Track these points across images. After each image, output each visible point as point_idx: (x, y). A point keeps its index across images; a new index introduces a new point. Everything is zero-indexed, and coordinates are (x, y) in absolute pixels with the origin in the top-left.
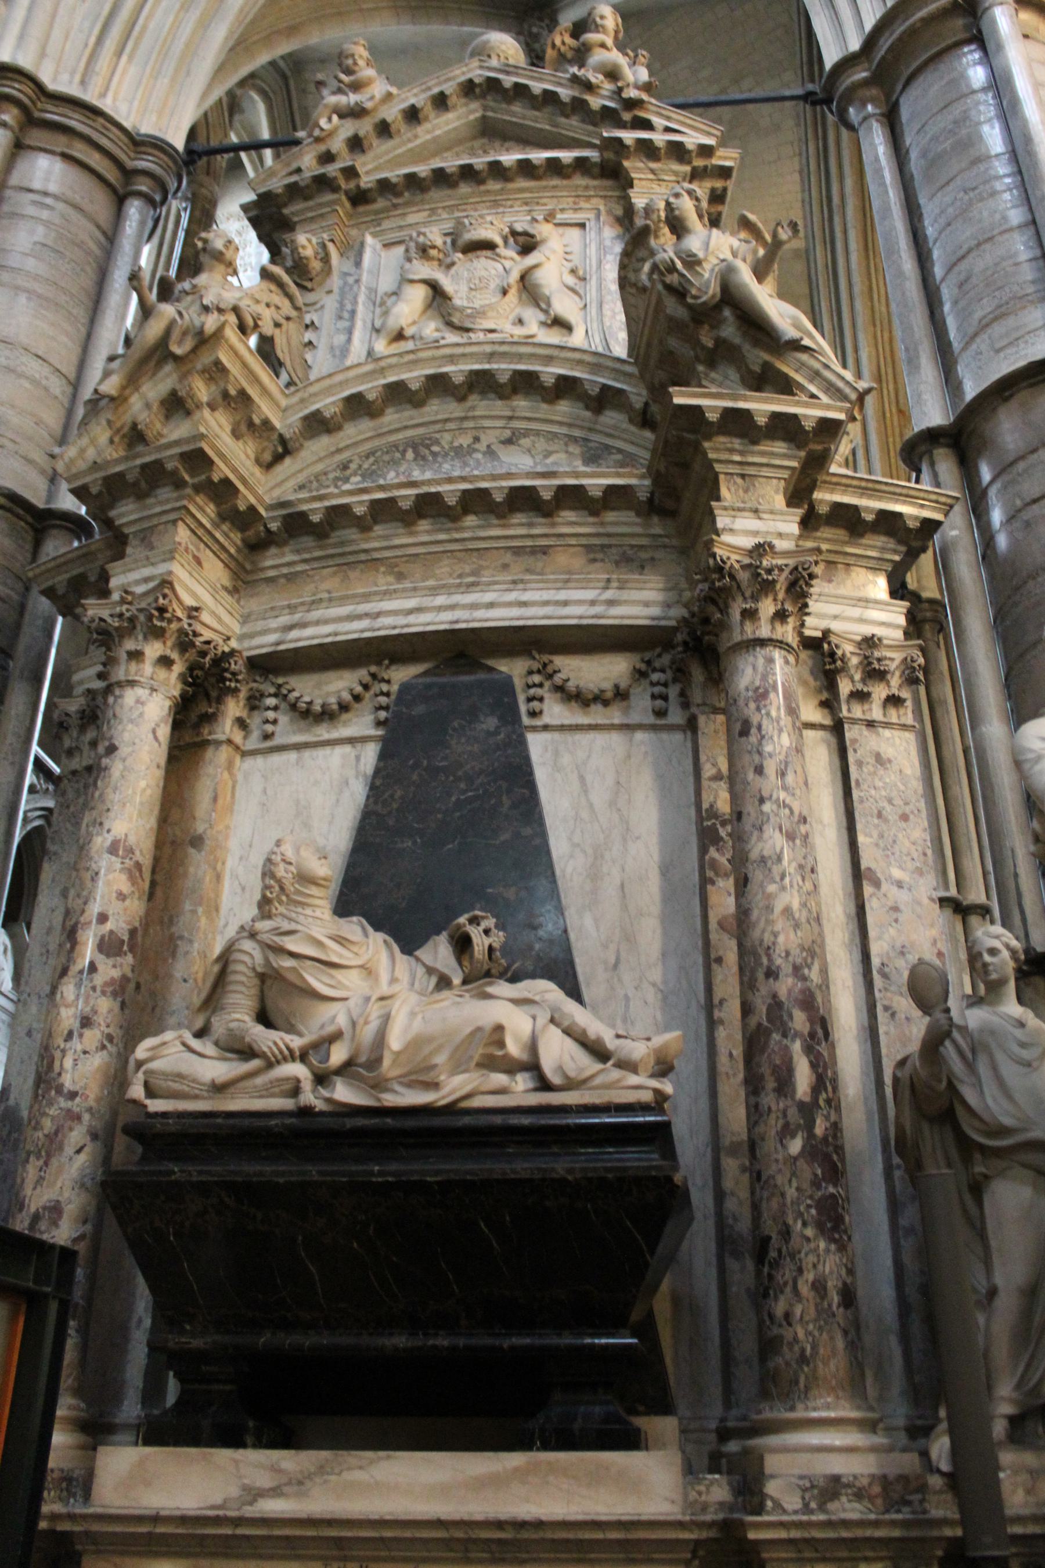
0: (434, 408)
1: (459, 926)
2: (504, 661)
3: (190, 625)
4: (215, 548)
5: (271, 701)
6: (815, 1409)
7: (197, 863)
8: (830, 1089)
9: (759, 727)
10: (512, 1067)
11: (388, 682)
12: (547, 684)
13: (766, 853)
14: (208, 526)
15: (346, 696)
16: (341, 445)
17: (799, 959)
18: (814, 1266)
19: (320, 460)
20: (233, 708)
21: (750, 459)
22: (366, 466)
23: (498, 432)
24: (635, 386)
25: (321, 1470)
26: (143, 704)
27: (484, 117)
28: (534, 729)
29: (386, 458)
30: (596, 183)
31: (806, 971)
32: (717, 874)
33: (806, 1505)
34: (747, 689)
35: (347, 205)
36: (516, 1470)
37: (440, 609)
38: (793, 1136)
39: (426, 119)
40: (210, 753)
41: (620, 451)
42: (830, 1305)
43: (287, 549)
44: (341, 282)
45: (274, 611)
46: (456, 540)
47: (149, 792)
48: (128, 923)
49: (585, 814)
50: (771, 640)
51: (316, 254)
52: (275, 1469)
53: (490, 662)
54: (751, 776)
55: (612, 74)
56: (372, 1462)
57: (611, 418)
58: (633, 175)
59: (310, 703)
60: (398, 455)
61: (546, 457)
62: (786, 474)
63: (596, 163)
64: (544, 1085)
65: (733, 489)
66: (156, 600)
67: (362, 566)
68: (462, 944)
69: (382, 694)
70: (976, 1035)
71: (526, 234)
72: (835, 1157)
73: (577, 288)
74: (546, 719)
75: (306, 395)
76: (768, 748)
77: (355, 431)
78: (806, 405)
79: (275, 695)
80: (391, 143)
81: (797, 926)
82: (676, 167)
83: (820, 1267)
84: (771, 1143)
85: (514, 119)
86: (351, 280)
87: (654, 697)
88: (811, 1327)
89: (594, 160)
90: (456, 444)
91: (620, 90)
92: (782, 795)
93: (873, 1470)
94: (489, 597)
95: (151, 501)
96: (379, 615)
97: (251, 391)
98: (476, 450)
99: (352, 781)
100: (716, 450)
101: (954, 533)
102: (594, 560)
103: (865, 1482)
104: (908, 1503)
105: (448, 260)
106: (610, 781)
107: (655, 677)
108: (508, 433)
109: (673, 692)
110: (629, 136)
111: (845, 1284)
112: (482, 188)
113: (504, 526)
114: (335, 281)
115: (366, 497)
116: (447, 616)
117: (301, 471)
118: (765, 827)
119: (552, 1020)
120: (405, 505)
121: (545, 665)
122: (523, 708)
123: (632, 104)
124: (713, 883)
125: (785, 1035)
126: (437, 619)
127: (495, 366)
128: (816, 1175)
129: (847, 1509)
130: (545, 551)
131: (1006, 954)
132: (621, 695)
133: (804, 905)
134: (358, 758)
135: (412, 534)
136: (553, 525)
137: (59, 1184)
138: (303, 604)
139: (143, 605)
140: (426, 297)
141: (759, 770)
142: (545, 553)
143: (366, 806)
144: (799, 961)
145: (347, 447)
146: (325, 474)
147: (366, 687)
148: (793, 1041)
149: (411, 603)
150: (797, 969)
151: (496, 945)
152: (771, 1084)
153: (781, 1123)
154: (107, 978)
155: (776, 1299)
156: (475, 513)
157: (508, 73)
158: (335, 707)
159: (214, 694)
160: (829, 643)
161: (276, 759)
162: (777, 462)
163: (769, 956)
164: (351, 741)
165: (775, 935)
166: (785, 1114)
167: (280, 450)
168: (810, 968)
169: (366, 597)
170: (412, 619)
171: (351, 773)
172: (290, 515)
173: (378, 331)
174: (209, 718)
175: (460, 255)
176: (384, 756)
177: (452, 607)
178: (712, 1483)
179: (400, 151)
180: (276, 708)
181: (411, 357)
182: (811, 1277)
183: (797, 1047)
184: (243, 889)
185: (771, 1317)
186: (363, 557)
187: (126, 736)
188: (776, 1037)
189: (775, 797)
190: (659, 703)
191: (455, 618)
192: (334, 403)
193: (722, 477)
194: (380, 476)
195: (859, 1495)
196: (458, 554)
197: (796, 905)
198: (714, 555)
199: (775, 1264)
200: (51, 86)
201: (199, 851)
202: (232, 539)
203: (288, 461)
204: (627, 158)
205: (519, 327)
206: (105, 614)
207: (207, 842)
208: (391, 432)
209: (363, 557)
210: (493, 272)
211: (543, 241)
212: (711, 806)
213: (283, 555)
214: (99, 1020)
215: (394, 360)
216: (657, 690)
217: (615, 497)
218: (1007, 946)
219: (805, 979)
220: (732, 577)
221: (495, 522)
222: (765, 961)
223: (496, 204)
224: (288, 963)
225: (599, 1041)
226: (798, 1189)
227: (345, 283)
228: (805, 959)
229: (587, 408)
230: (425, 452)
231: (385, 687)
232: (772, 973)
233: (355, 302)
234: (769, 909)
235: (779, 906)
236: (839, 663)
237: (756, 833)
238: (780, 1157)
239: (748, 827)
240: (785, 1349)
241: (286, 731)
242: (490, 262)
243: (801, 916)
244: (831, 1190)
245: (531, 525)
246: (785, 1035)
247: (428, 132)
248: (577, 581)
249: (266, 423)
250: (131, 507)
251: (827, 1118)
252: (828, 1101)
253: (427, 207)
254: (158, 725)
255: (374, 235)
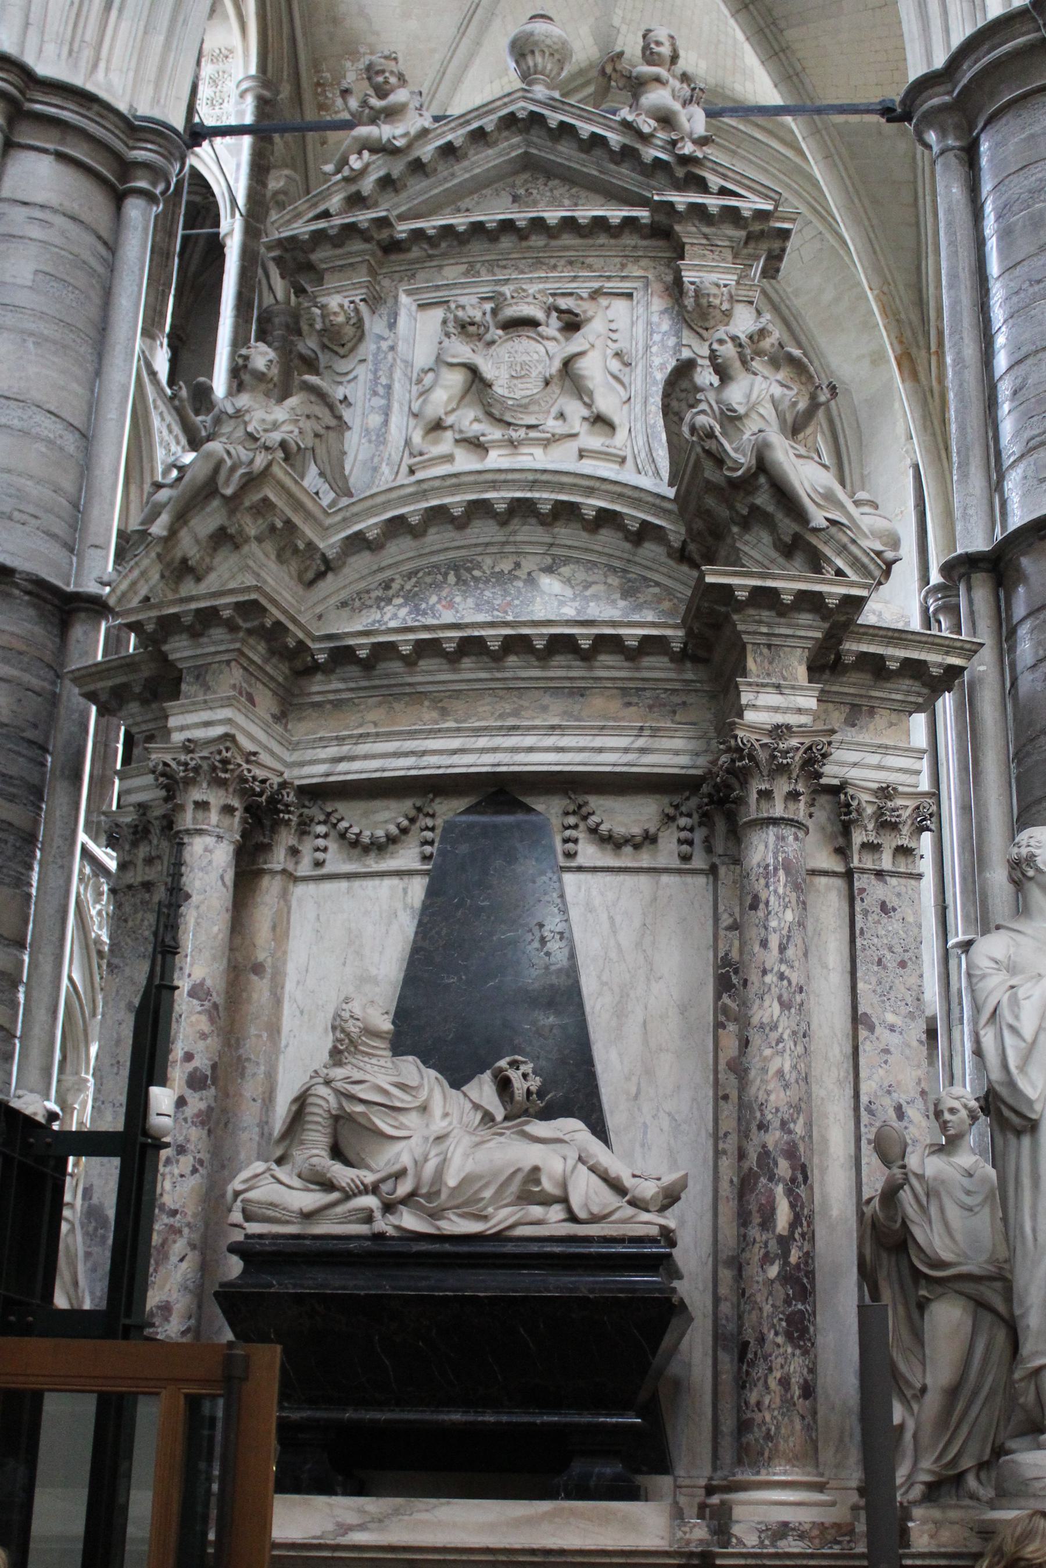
0: (476, 530)
1: (501, 1070)
2: (542, 799)
3: (249, 771)
4: (266, 680)
5: (321, 829)
6: (775, 1474)
7: (260, 989)
8: (805, 1223)
9: (767, 903)
10: (547, 1201)
11: (433, 816)
12: (582, 826)
13: (765, 1020)
14: (259, 661)
15: (393, 830)
16: (383, 564)
17: (785, 1113)
18: (782, 1367)
19: (363, 578)
20: (286, 838)
21: (777, 631)
22: (408, 587)
23: (538, 558)
24: (673, 523)
25: (397, 1512)
26: (211, 851)
27: (526, 153)
28: (569, 869)
29: (428, 579)
30: (645, 243)
31: (792, 1125)
32: (728, 1020)
33: (762, 1542)
34: (759, 866)
35: (379, 253)
36: (546, 1513)
37: (483, 751)
38: (772, 1263)
39: (465, 156)
40: (266, 881)
41: (657, 584)
42: (792, 1397)
43: (332, 677)
44: (373, 347)
45: (323, 742)
46: (498, 679)
47: (220, 936)
48: (210, 1059)
49: (613, 955)
50: (783, 819)
51: (349, 319)
52: (361, 1511)
53: (528, 800)
54: (757, 948)
55: (666, 120)
56: (435, 1507)
57: (651, 550)
58: (685, 240)
59: (358, 835)
60: (440, 577)
61: (586, 588)
62: (809, 644)
63: (645, 225)
64: (573, 1218)
65: (758, 660)
66: (220, 752)
67: (407, 699)
68: (504, 1085)
69: (427, 828)
70: (930, 1182)
71: (569, 312)
72: (805, 1281)
73: (621, 376)
74: (580, 860)
75: (348, 514)
76: (773, 924)
77: (400, 549)
78: (831, 582)
79: (325, 822)
80: (425, 183)
81: (786, 1086)
82: (731, 231)
83: (786, 1367)
84: (753, 1270)
85: (559, 160)
86: (385, 345)
87: (680, 842)
88: (776, 1413)
89: (643, 221)
90: (497, 569)
91: (674, 143)
92: (783, 968)
93: (817, 1520)
94: (529, 741)
95: (205, 640)
96: (424, 753)
97: (296, 520)
98: (517, 578)
99: (400, 913)
100: (744, 622)
101: (982, 668)
102: (629, 704)
103: (807, 1527)
104: (839, 1543)
105: (488, 337)
106: (637, 923)
107: (683, 821)
108: (549, 560)
109: (698, 836)
110: (681, 200)
111: (806, 1381)
112: (524, 244)
113: (543, 668)
114: (368, 348)
115: (411, 636)
116: (489, 758)
117: (345, 587)
118: (766, 997)
119: (580, 1159)
120: (450, 647)
121: (580, 807)
122: (559, 847)
123: (686, 160)
124: (724, 1027)
125: (771, 1179)
126: (479, 762)
127: (537, 495)
128: (788, 1295)
129: (791, 1545)
130: (582, 692)
131: (964, 1113)
132: (650, 839)
133: (794, 1067)
134: (405, 891)
135: (455, 671)
136: (591, 668)
137: (168, 1287)
138: (350, 737)
139: (205, 754)
140: (465, 382)
141: (764, 944)
142: (582, 695)
143: (415, 941)
144: (786, 1116)
145: (390, 566)
146: (368, 592)
147: (412, 821)
148: (777, 1184)
149: (455, 743)
150: (784, 1124)
151: (533, 1089)
152: (756, 1219)
153: (763, 1251)
154: (196, 1111)
155: (751, 1390)
156: (516, 654)
157: (554, 109)
158: (383, 840)
159: (267, 822)
160: (846, 794)
161: (328, 886)
162: (802, 633)
163: (761, 1111)
164: (399, 873)
165: (768, 1093)
166: (766, 1244)
167: (323, 568)
168: (795, 1122)
169: (412, 734)
170: (456, 759)
171: (399, 905)
172: (337, 648)
173: (416, 416)
174: (265, 848)
175: (500, 332)
176: (431, 892)
177: (495, 750)
178: (695, 1526)
179: (436, 191)
180: (326, 836)
181: (454, 481)
182: (778, 1374)
183: (780, 1190)
184: (302, 1012)
185: (746, 1403)
186: (408, 690)
187: (197, 884)
188: (763, 1180)
189: (776, 969)
190: (685, 848)
191: (496, 761)
192: (376, 524)
193: (749, 647)
194: (422, 599)
195: (802, 1536)
196: (501, 693)
197: (787, 1068)
198: (736, 737)
199: (752, 1364)
200: (43, 70)
201: (262, 978)
202: (279, 671)
203: (330, 576)
204: (679, 222)
205: (560, 422)
206: (168, 758)
207: (269, 970)
208: (432, 553)
209: (408, 690)
210: (536, 357)
211: (589, 320)
212: (727, 954)
213: (330, 682)
214: (191, 1147)
215: (437, 483)
216: (684, 835)
217: (650, 645)
218: (965, 1106)
219: (790, 1132)
220: (752, 757)
221: (536, 663)
222: (758, 1114)
223: (538, 263)
224: (360, 1108)
225: (618, 1179)
226: (773, 1306)
227: (379, 348)
228: (792, 1115)
229: (627, 539)
230: (466, 575)
231: (430, 822)
232: (763, 1127)
233: (391, 377)
234: (764, 1070)
235: (773, 1067)
236: (854, 815)
237: (758, 1001)
238: (760, 1279)
239: (751, 996)
240: (756, 1429)
241: (336, 861)
242: (532, 342)
243: (791, 1077)
244: (800, 1306)
245: (569, 667)
246: (771, 1179)
247: (466, 170)
248: (613, 728)
249: (310, 545)
250: (185, 643)
251: (800, 1248)
252: (803, 1235)
253: (464, 260)
254: (225, 871)
255: (409, 293)
